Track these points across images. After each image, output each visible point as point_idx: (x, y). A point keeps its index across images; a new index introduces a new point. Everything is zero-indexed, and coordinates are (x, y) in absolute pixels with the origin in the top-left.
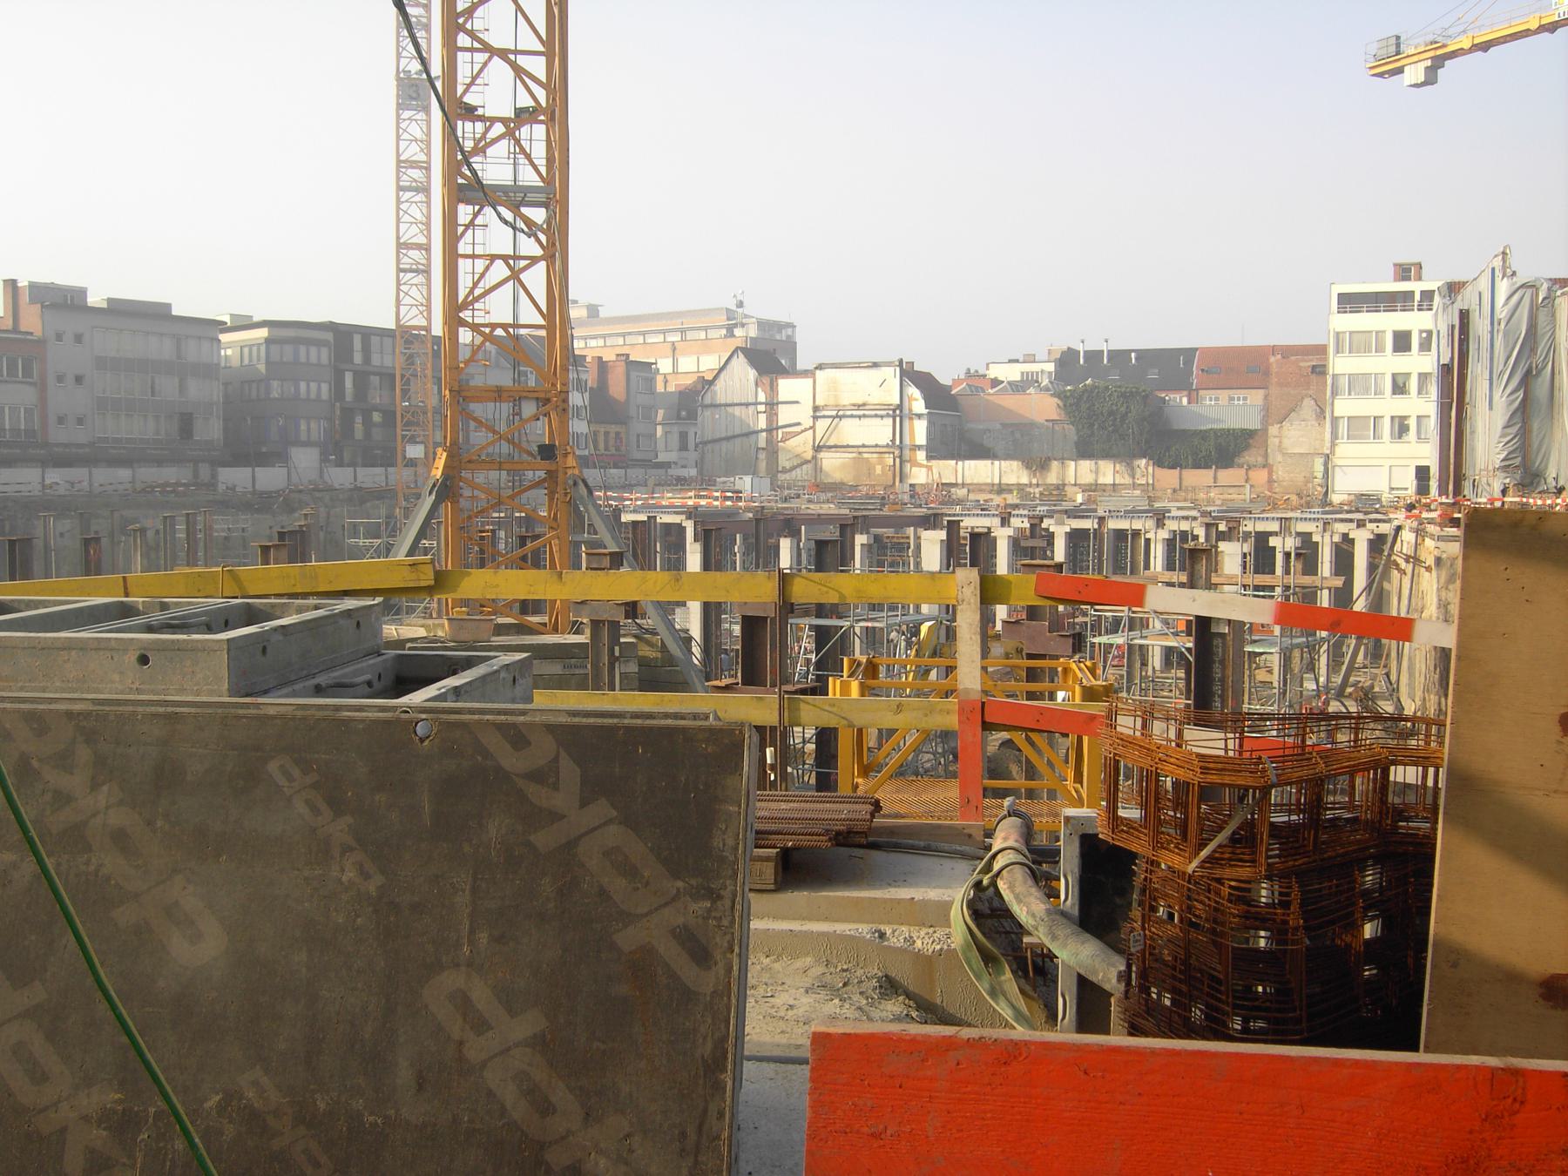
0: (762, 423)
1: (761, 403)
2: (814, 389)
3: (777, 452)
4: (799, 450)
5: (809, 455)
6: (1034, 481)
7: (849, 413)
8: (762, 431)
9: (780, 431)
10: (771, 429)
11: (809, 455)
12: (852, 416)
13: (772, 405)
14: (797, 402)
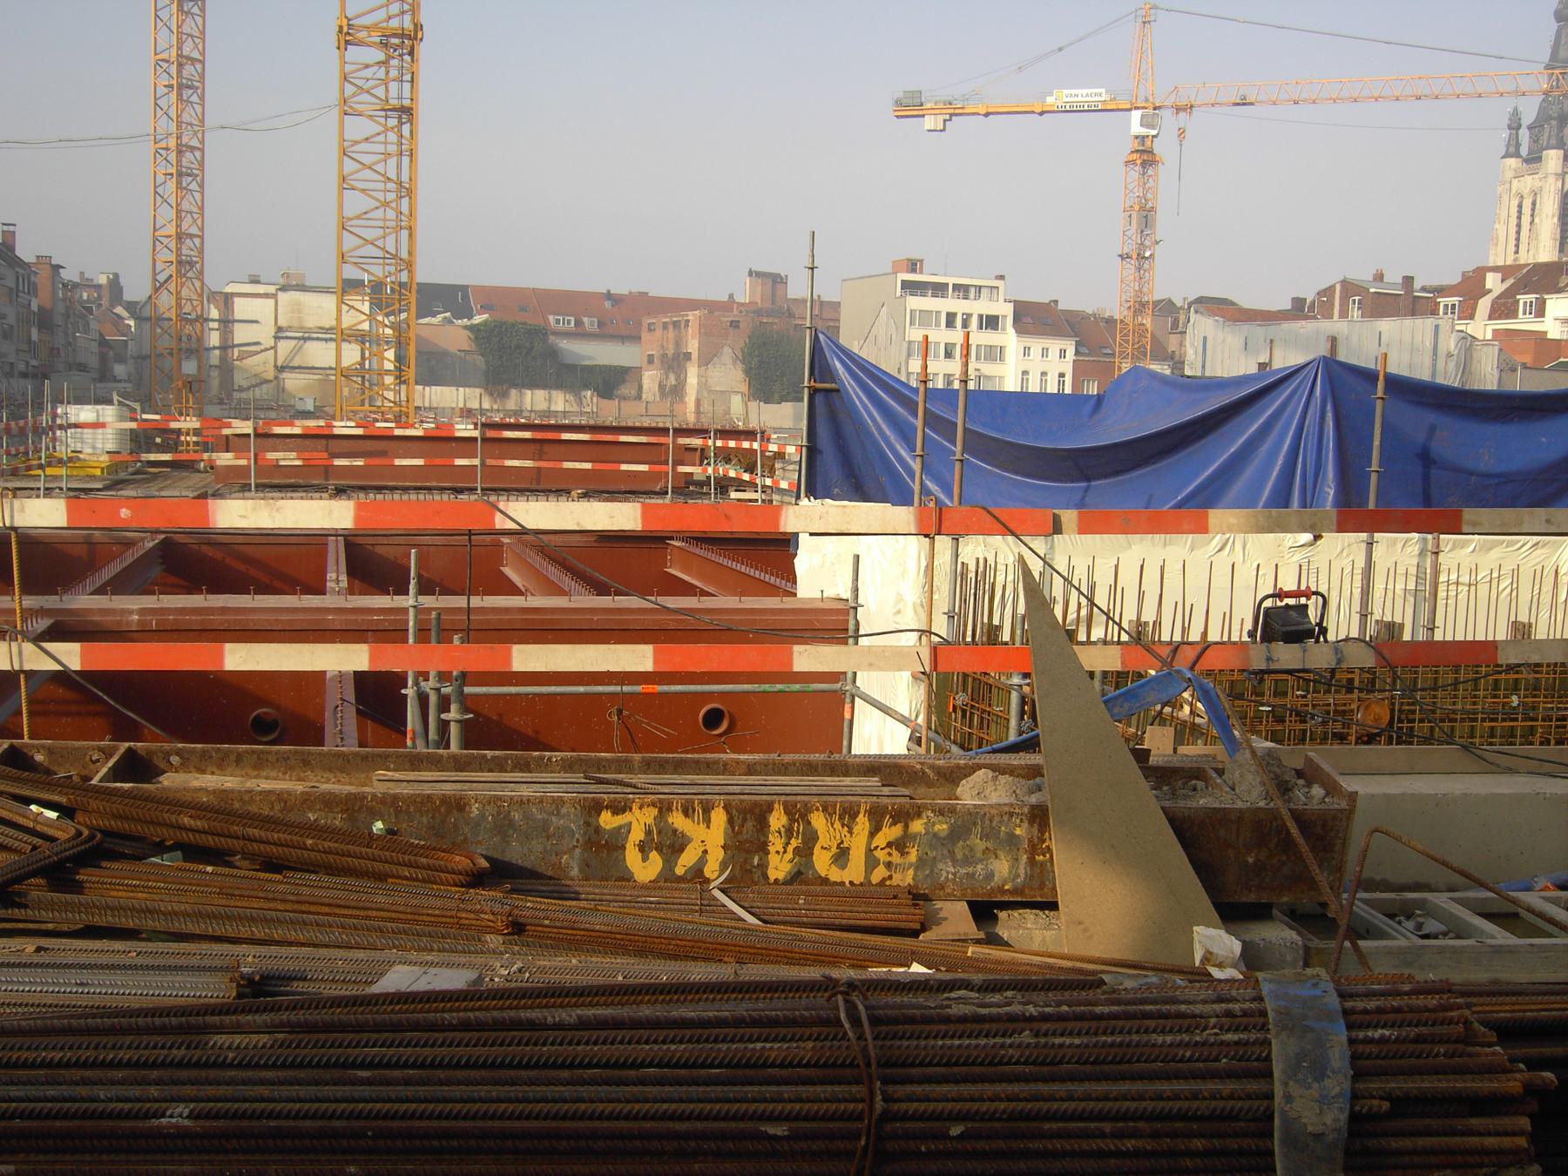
0: (214, 339)
1: (213, 320)
2: (276, 310)
3: (232, 370)
4: (259, 369)
5: (270, 375)
6: (495, 407)
7: (315, 335)
8: (214, 348)
9: (236, 351)
10: (226, 347)
11: (270, 375)
12: (318, 339)
13: (227, 323)
14: (256, 322)
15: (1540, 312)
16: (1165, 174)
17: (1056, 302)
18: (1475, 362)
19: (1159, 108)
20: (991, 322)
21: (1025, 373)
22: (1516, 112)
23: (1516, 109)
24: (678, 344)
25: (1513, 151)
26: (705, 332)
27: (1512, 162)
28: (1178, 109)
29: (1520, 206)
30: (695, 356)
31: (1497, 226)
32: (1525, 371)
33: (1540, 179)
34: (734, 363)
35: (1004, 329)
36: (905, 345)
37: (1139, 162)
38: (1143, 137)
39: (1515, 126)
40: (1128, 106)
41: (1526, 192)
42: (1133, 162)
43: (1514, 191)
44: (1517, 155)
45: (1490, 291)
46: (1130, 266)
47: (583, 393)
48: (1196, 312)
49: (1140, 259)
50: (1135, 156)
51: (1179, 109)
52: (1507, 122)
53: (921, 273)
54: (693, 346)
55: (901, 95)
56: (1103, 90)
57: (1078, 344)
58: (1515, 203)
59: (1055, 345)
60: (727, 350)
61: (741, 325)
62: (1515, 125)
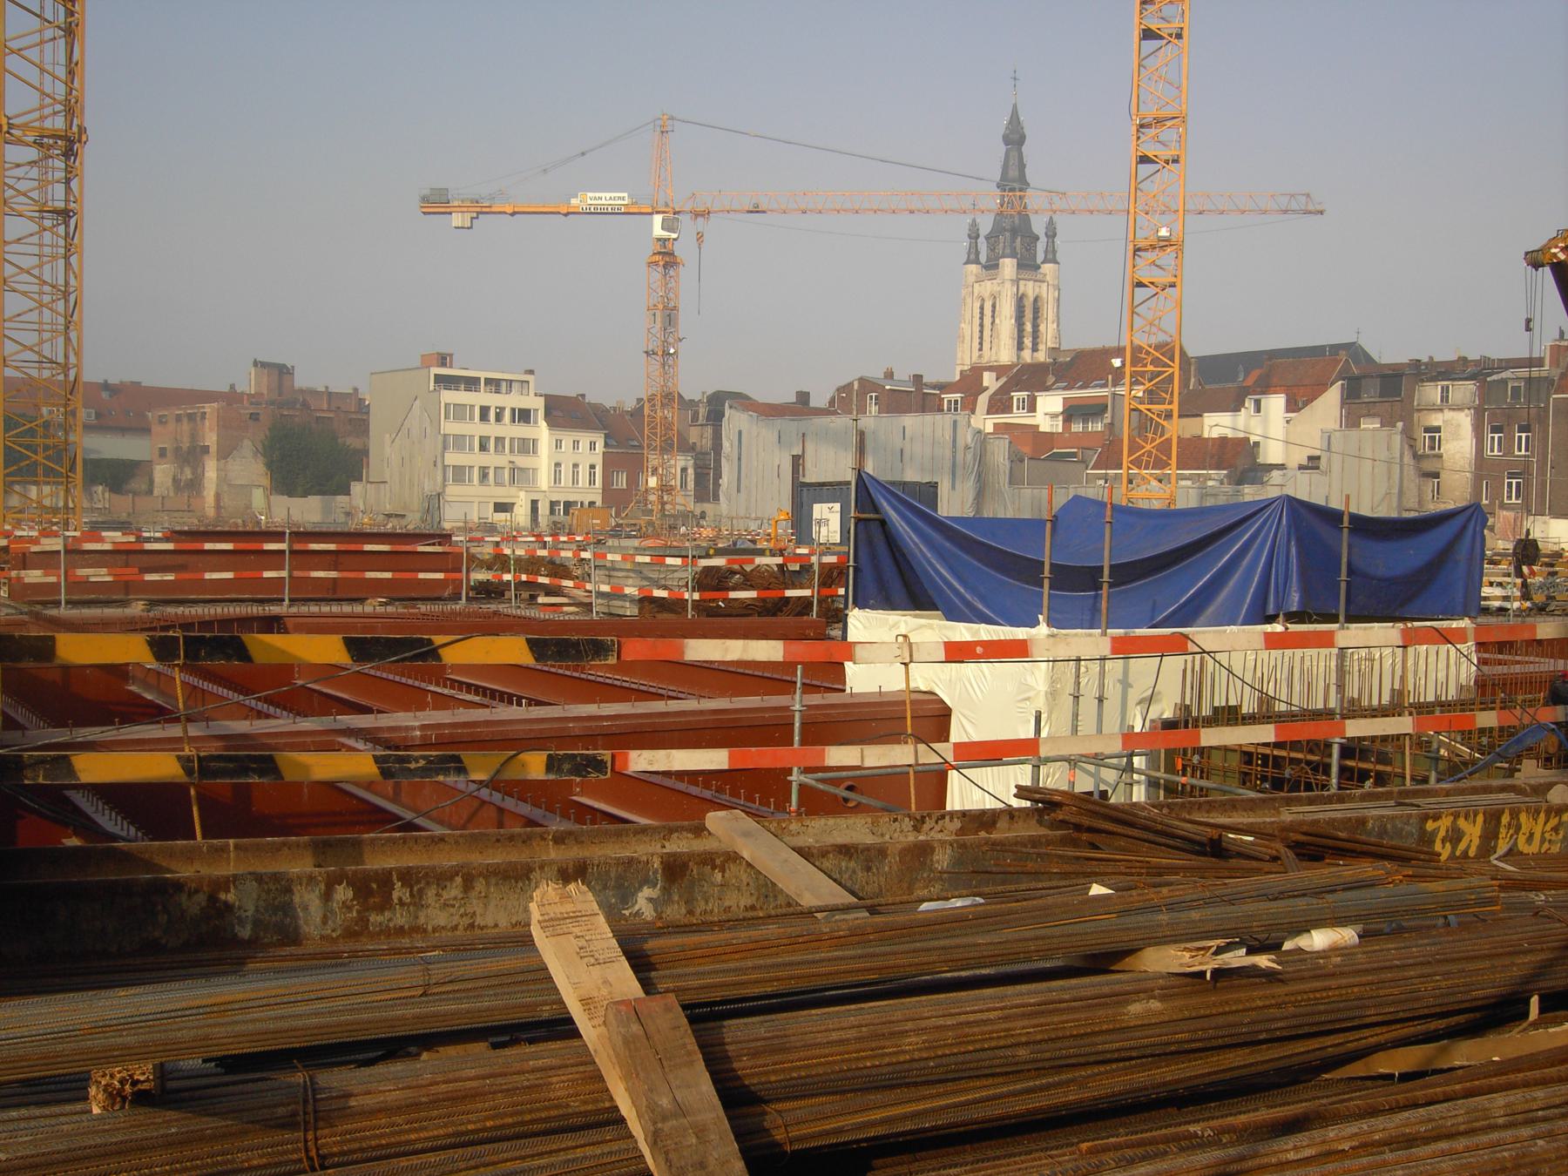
15: (1032, 408)
16: (685, 275)
17: (583, 396)
18: (988, 454)
19: (678, 213)
20: (524, 416)
21: (558, 465)
22: (974, 224)
23: (974, 220)
24: (194, 436)
25: (973, 258)
26: (224, 425)
27: (973, 268)
28: (697, 215)
29: (982, 308)
30: (213, 449)
31: (963, 325)
32: (1032, 462)
33: (999, 284)
34: (255, 456)
35: (536, 422)
36: (440, 438)
37: (661, 263)
38: (665, 240)
39: (974, 236)
40: (650, 210)
41: (986, 295)
42: (656, 263)
43: (976, 295)
44: (977, 262)
45: (987, 388)
46: (655, 363)
47: (94, 489)
48: (731, 407)
49: (664, 355)
50: (657, 258)
51: (697, 215)
52: (967, 232)
53: (451, 367)
54: (211, 439)
55: (427, 192)
56: (626, 195)
57: (607, 436)
58: (977, 305)
59: (585, 439)
60: (247, 443)
61: (261, 418)
62: (974, 235)
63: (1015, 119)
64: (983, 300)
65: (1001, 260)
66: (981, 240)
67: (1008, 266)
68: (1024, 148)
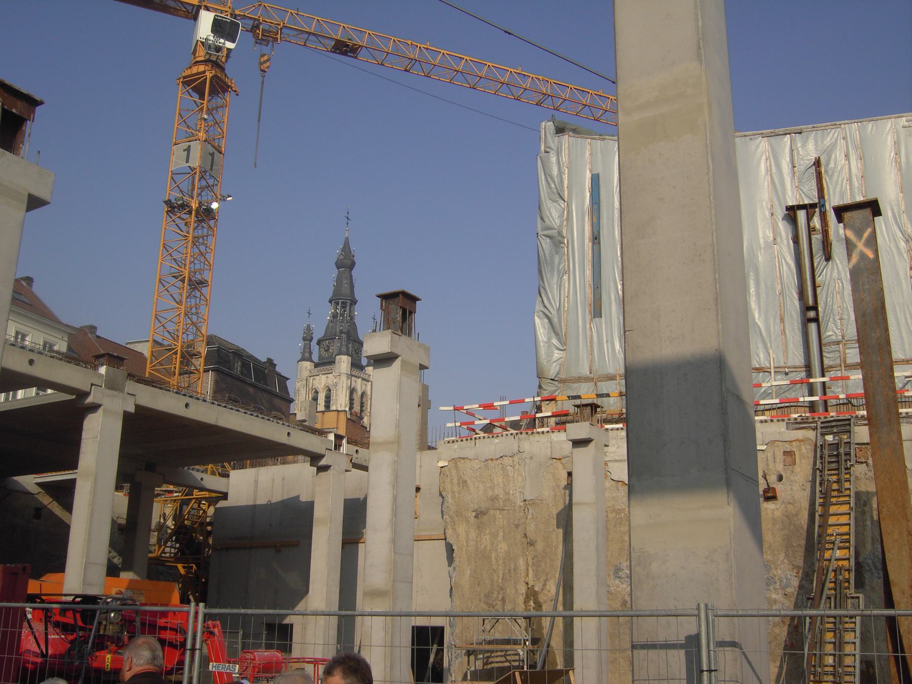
23: (309, 326)
25: (306, 356)
27: (307, 365)
33: (336, 377)
39: (308, 338)
44: (310, 360)
62: (309, 338)
63: (346, 248)
64: (317, 392)
65: (337, 357)
66: (314, 343)
67: (344, 362)
68: (354, 273)
